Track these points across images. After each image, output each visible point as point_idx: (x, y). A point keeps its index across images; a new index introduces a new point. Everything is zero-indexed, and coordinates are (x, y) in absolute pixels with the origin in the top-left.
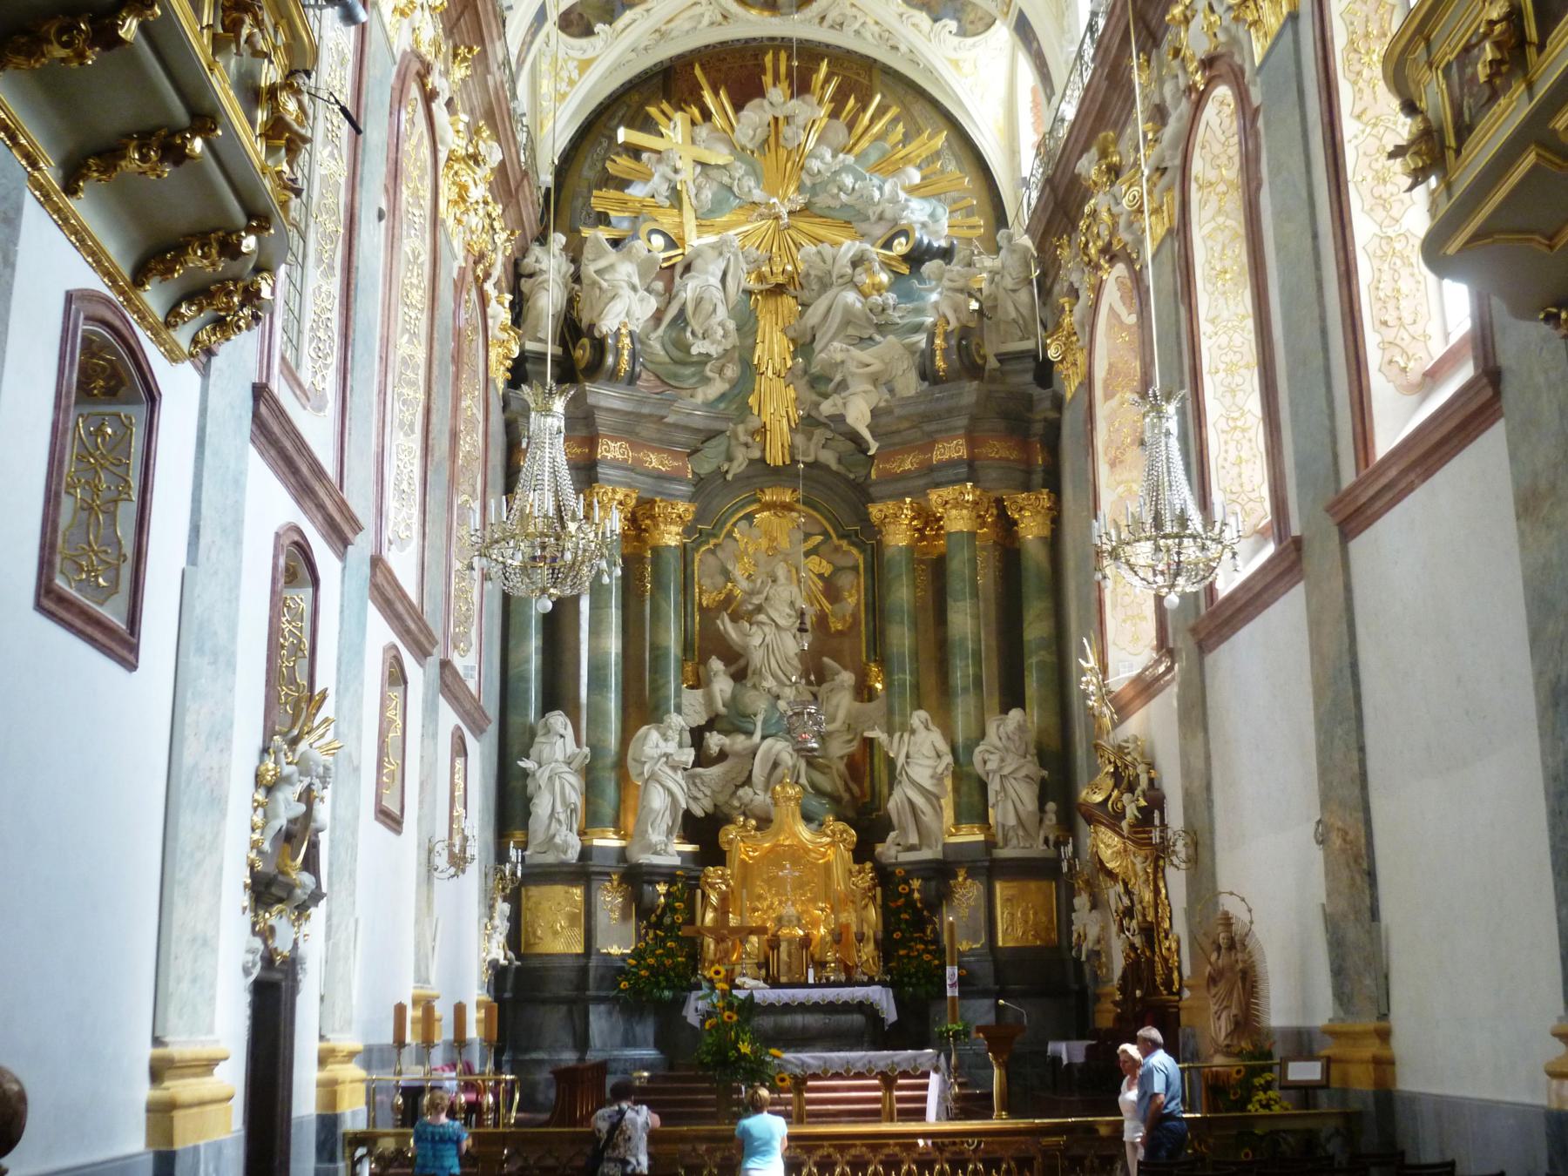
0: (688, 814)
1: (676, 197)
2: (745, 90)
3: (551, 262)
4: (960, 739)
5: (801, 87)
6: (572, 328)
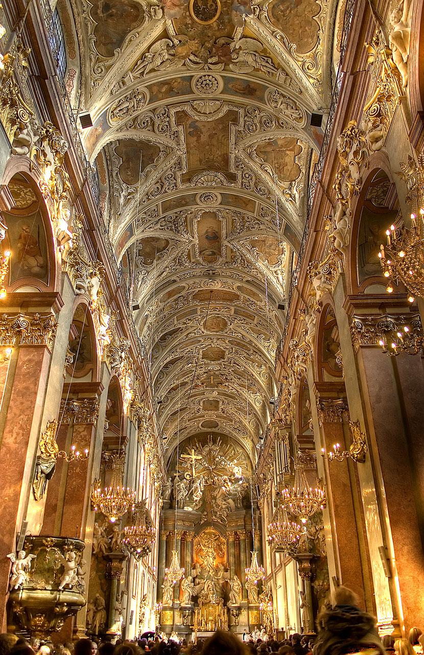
0: (192, 596)
1: (191, 465)
2: (204, 443)
3: (169, 484)
4: (243, 582)
5: (214, 442)
6: (172, 497)
